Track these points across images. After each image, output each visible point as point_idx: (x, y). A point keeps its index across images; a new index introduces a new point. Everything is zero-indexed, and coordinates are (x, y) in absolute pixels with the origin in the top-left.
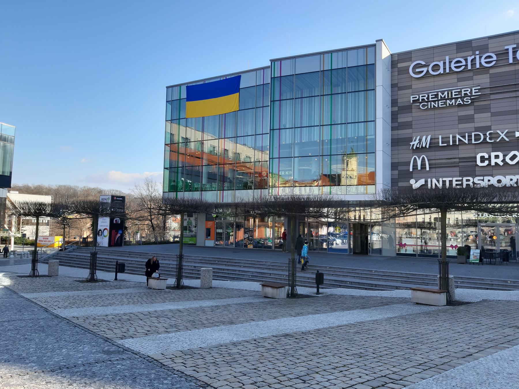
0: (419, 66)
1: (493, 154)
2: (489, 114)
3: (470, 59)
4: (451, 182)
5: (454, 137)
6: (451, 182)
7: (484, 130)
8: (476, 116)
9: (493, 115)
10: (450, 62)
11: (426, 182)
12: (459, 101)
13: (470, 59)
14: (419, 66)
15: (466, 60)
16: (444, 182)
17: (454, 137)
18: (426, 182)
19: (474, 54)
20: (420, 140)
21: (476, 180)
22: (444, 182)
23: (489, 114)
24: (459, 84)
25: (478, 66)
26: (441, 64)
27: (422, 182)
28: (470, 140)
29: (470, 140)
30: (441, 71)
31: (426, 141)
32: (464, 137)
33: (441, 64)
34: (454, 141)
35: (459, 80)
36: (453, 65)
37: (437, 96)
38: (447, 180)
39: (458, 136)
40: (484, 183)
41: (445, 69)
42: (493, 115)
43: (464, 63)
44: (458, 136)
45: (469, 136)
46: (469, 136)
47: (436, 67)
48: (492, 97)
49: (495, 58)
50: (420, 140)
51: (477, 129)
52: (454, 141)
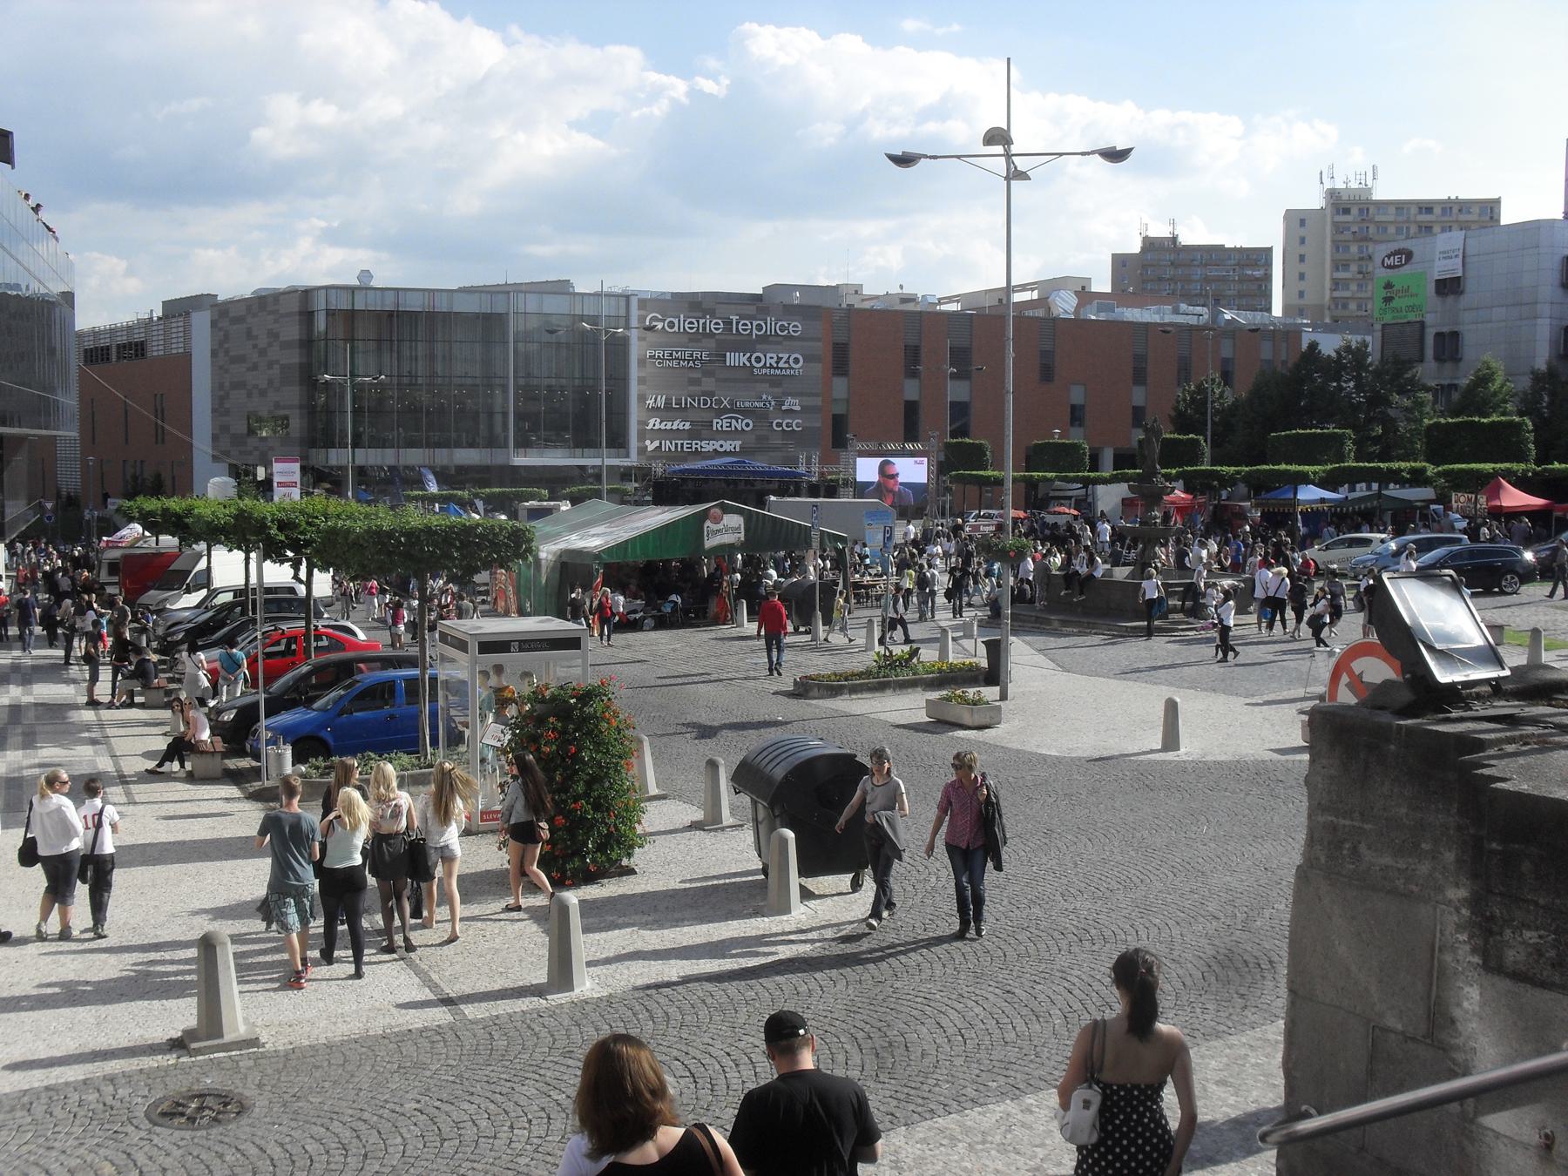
2: (713, 380)
3: (701, 321)
4: (682, 444)
5: (686, 400)
6: (682, 444)
7: (711, 394)
8: (704, 379)
9: (717, 380)
10: (684, 321)
11: (661, 443)
13: (701, 321)
15: (698, 322)
16: (676, 444)
17: (686, 400)
18: (661, 443)
19: (704, 317)
20: (656, 399)
22: (676, 444)
23: (713, 380)
24: (690, 345)
25: (708, 331)
26: (676, 321)
27: (656, 443)
28: (699, 404)
29: (699, 404)
30: (676, 329)
32: (694, 400)
33: (676, 321)
34: (686, 404)
35: (691, 340)
36: (687, 326)
37: (671, 355)
38: (679, 442)
39: (689, 399)
41: (679, 328)
43: (696, 325)
44: (689, 399)
45: (699, 400)
46: (699, 400)
47: (671, 325)
49: (722, 326)
50: (656, 399)
52: (686, 404)
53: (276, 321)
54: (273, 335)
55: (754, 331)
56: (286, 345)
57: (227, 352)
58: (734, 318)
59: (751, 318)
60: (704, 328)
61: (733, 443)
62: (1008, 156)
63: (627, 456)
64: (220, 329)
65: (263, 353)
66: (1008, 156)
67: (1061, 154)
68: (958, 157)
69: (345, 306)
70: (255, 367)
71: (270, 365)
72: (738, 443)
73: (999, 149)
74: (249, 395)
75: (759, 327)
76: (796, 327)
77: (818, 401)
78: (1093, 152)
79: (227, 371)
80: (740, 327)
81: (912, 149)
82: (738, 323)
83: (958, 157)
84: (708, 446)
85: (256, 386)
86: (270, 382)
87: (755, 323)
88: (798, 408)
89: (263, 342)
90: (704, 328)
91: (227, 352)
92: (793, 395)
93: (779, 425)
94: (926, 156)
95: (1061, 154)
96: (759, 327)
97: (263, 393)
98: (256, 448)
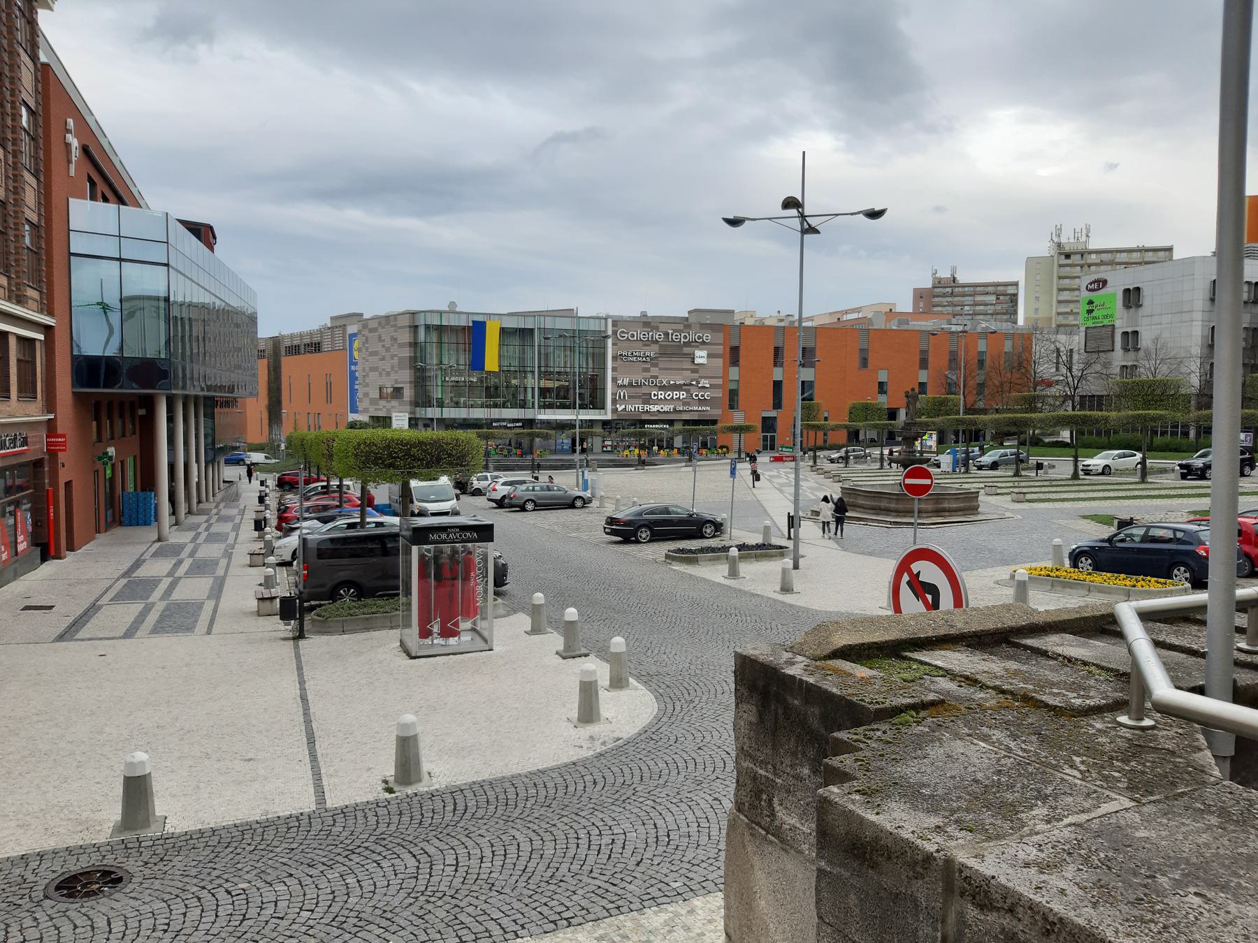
0: (623, 332)
1: (660, 393)
3: (651, 334)
12: (644, 359)
13: (651, 334)
14: (623, 332)
21: (651, 407)
27: (623, 407)
30: (635, 338)
31: (626, 382)
35: (644, 345)
40: (655, 409)
42: (660, 369)
47: (633, 336)
48: (660, 359)
51: (652, 377)
53: (395, 331)
54: (394, 339)
55: (682, 340)
56: (401, 346)
57: (367, 348)
58: (670, 332)
59: (680, 331)
60: (652, 337)
61: (669, 407)
62: (803, 217)
63: (606, 414)
64: (364, 335)
65: (388, 350)
66: (803, 217)
67: (837, 215)
68: (769, 219)
69: (437, 322)
70: (383, 359)
71: (393, 357)
72: (672, 407)
73: (794, 212)
74: (381, 375)
75: (685, 337)
76: (708, 336)
77: (720, 381)
78: (859, 213)
79: (367, 361)
80: (674, 337)
81: (740, 215)
82: (672, 335)
83: (769, 219)
84: (654, 408)
85: (384, 370)
86: (392, 368)
87: (682, 335)
88: (708, 386)
89: (388, 344)
90: (652, 337)
91: (367, 348)
92: (705, 378)
93: (697, 395)
94: (749, 219)
95: (837, 215)
96: (685, 337)
97: (388, 374)
98: (384, 407)
